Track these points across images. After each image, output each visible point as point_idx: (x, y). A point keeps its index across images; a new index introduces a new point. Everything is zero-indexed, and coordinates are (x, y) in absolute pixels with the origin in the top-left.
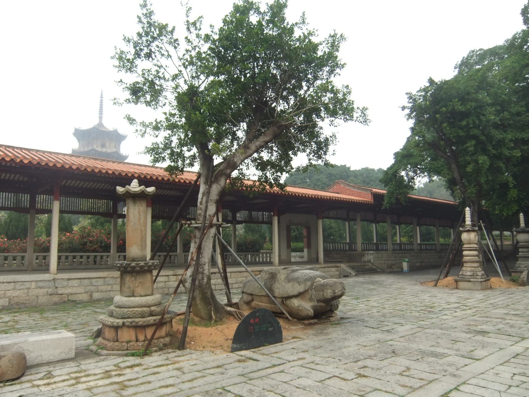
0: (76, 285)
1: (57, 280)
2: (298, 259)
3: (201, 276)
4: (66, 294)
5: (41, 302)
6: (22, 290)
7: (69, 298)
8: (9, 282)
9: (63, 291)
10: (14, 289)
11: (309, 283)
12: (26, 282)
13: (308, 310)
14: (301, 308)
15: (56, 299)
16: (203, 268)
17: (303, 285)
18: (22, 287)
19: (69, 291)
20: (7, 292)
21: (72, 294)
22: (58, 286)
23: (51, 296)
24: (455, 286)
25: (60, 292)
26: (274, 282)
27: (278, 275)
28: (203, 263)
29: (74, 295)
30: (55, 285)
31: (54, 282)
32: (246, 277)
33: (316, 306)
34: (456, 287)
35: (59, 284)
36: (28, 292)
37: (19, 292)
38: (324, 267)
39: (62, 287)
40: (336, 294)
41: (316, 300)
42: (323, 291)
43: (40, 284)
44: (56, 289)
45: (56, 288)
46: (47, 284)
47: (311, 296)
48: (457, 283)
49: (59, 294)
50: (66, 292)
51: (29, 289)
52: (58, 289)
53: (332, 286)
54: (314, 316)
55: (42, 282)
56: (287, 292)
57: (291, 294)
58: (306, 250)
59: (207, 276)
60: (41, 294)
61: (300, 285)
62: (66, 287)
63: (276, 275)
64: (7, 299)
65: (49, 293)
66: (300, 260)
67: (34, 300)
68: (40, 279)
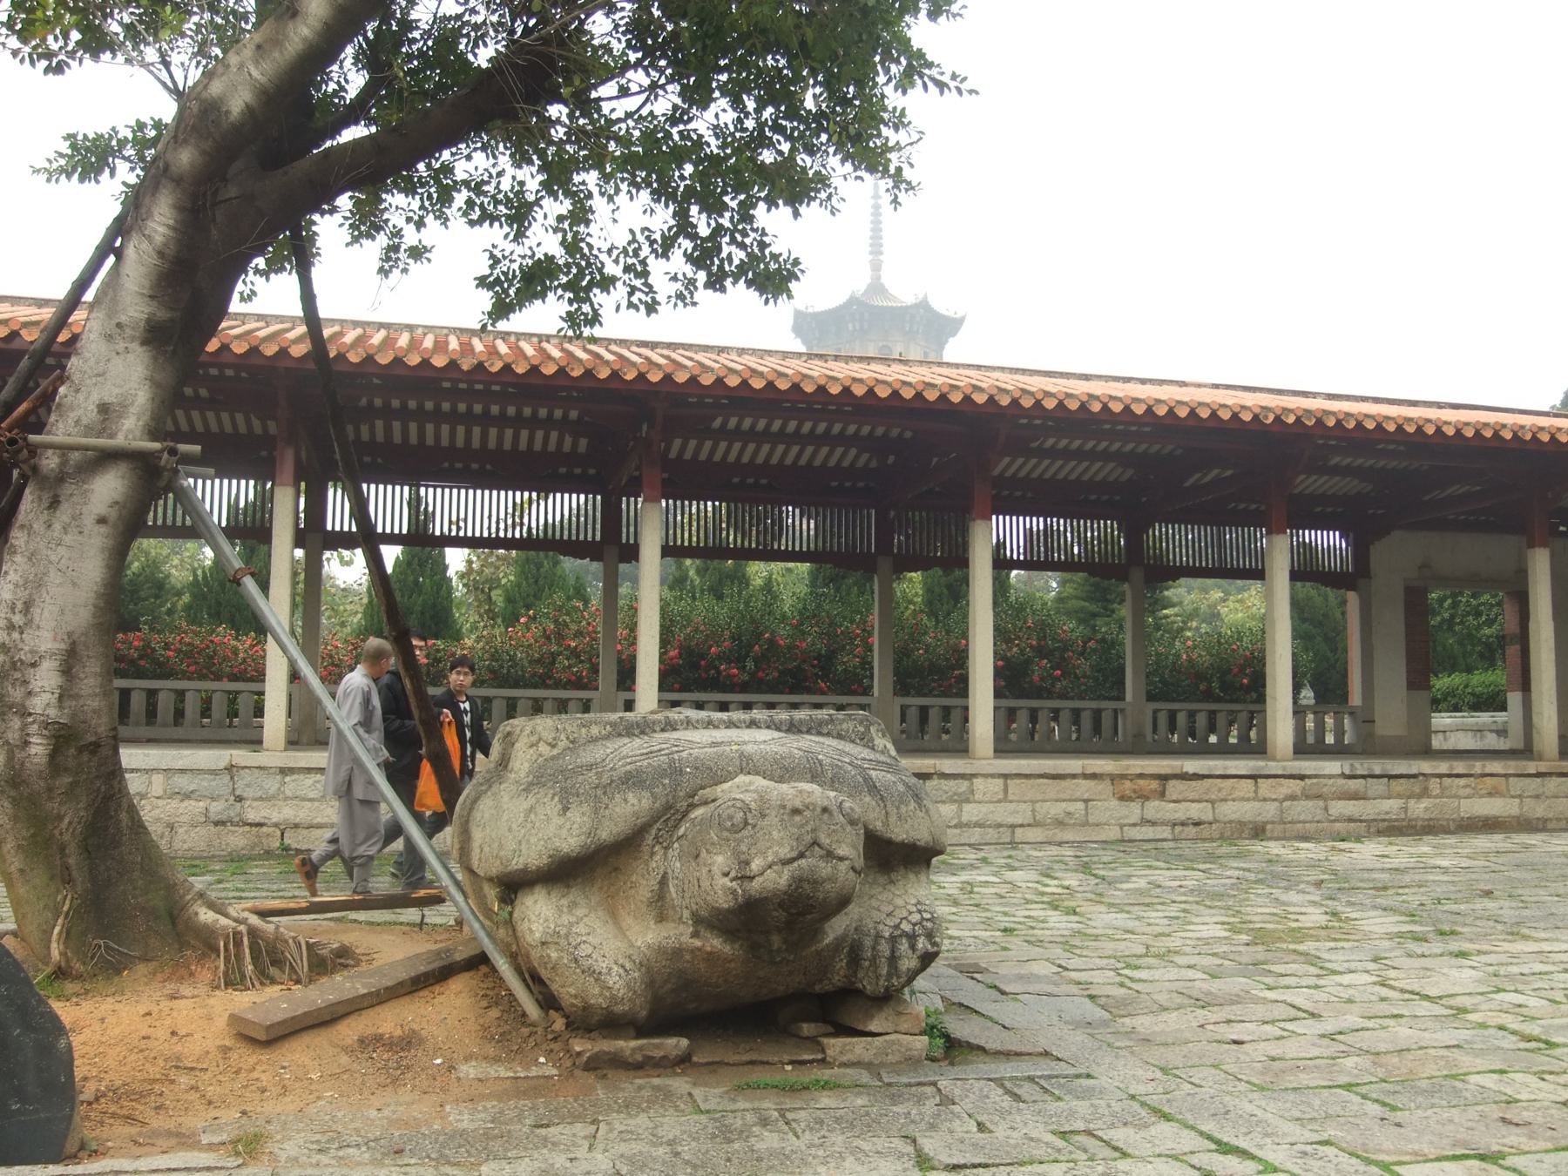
0: (311, 795)
1: (242, 772)
2: (1465, 742)
3: (16, 723)
4: (276, 825)
5: (185, 846)
7: (287, 841)
9: (264, 813)
11: (630, 807)
13: (590, 971)
14: (554, 955)
15: (237, 840)
16: (25, 682)
17: (585, 807)
21: (296, 826)
22: (245, 795)
23: (220, 828)
25: (252, 816)
28: (28, 658)
29: (305, 832)
30: (234, 789)
31: (232, 778)
32: (1086, 801)
33: (677, 952)
35: (248, 786)
38: (1539, 775)
39: (260, 799)
40: (756, 884)
41: (686, 914)
43: (183, 782)
45: (239, 799)
46: (204, 783)
47: (663, 882)
49: (251, 825)
50: (276, 817)
53: (735, 829)
54: (652, 1014)
58: (1514, 699)
59: (46, 725)
60: (184, 819)
61: (566, 809)
62: (273, 797)
65: (213, 817)
66: (1503, 744)
68: (180, 764)
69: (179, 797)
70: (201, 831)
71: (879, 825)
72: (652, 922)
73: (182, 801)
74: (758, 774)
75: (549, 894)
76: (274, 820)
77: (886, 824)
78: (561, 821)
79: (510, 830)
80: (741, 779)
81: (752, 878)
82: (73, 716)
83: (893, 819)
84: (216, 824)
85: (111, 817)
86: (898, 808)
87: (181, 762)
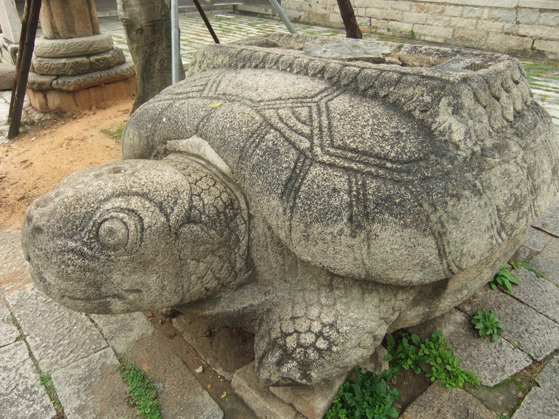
0: (552, 24)
1: (522, 10)
4: (531, 37)
5: (492, 42)
6: (470, 20)
7: (535, 45)
8: (457, 5)
9: (527, 31)
10: (461, 16)
12: (477, 6)
15: (513, 42)
18: (470, 15)
19: (536, 31)
20: (453, 19)
21: (541, 38)
22: (521, 21)
23: (507, 36)
25: (522, 32)
29: (544, 42)
30: (516, 18)
31: (517, 12)
35: (523, 17)
36: (477, 23)
37: (466, 21)
39: (527, 24)
43: (496, 13)
44: (517, 26)
45: (518, 23)
49: (520, 36)
50: (532, 33)
51: (479, 18)
52: (521, 25)
55: (499, 10)
60: (493, 30)
64: (451, 30)
65: (506, 30)
67: (483, 37)
69: (493, 20)
70: (499, 36)
71: (282, 235)
73: (494, 22)
74: (206, 138)
76: (531, 35)
77: (289, 236)
80: (195, 139)
82: (131, 15)
83: (296, 235)
84: (506, 34)
85: (152, 64)
86: (307, 225)
87: (497, 4)
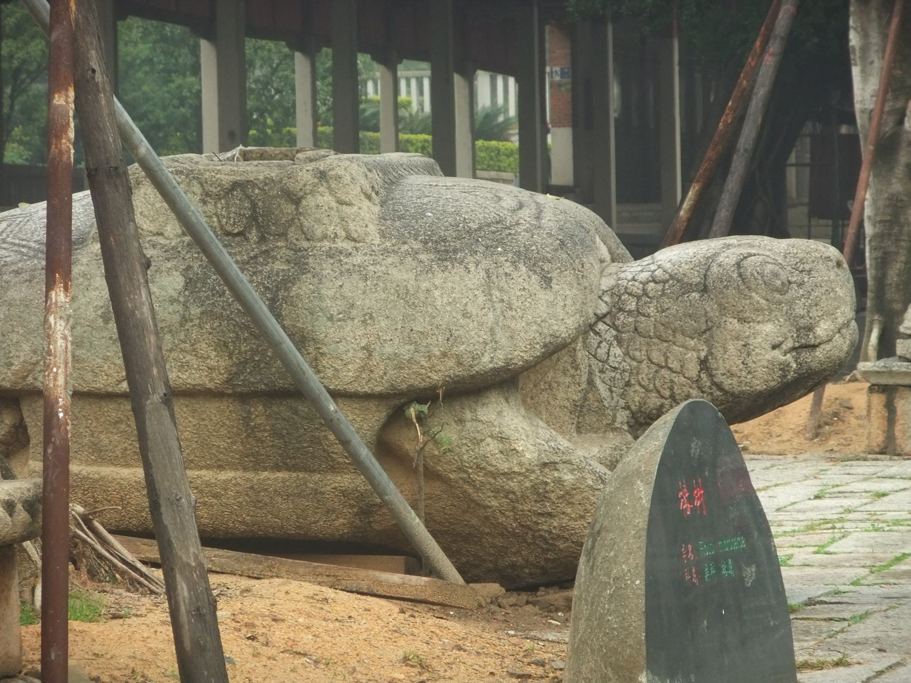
14: (568, 478)
24: (876, 431)
26: (300, 262)
27: (309, 202)
34: (878, 437)
41: (622, 416)
42: (707, 332)
48: (890, 407)
56: (451, 338)
57: (487, 361)
63: (296, 200)
72: (575, 434)
75: (507, 400)
78: (548, 296)
79: (466, 315)
81: (814, 347)
